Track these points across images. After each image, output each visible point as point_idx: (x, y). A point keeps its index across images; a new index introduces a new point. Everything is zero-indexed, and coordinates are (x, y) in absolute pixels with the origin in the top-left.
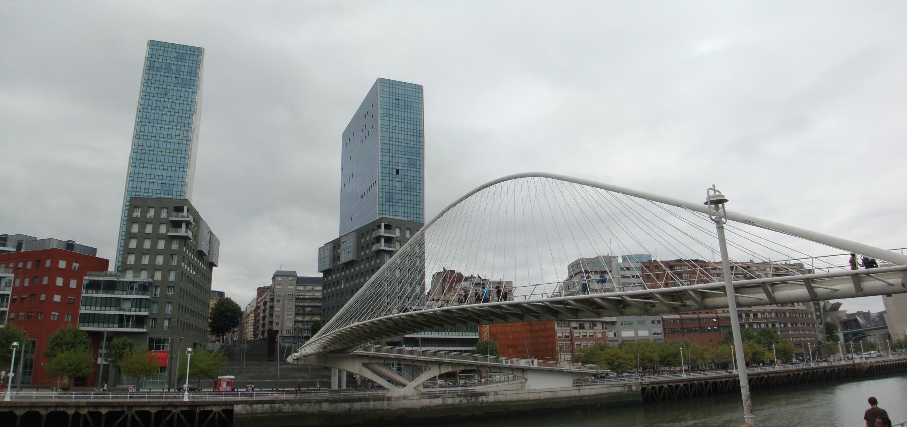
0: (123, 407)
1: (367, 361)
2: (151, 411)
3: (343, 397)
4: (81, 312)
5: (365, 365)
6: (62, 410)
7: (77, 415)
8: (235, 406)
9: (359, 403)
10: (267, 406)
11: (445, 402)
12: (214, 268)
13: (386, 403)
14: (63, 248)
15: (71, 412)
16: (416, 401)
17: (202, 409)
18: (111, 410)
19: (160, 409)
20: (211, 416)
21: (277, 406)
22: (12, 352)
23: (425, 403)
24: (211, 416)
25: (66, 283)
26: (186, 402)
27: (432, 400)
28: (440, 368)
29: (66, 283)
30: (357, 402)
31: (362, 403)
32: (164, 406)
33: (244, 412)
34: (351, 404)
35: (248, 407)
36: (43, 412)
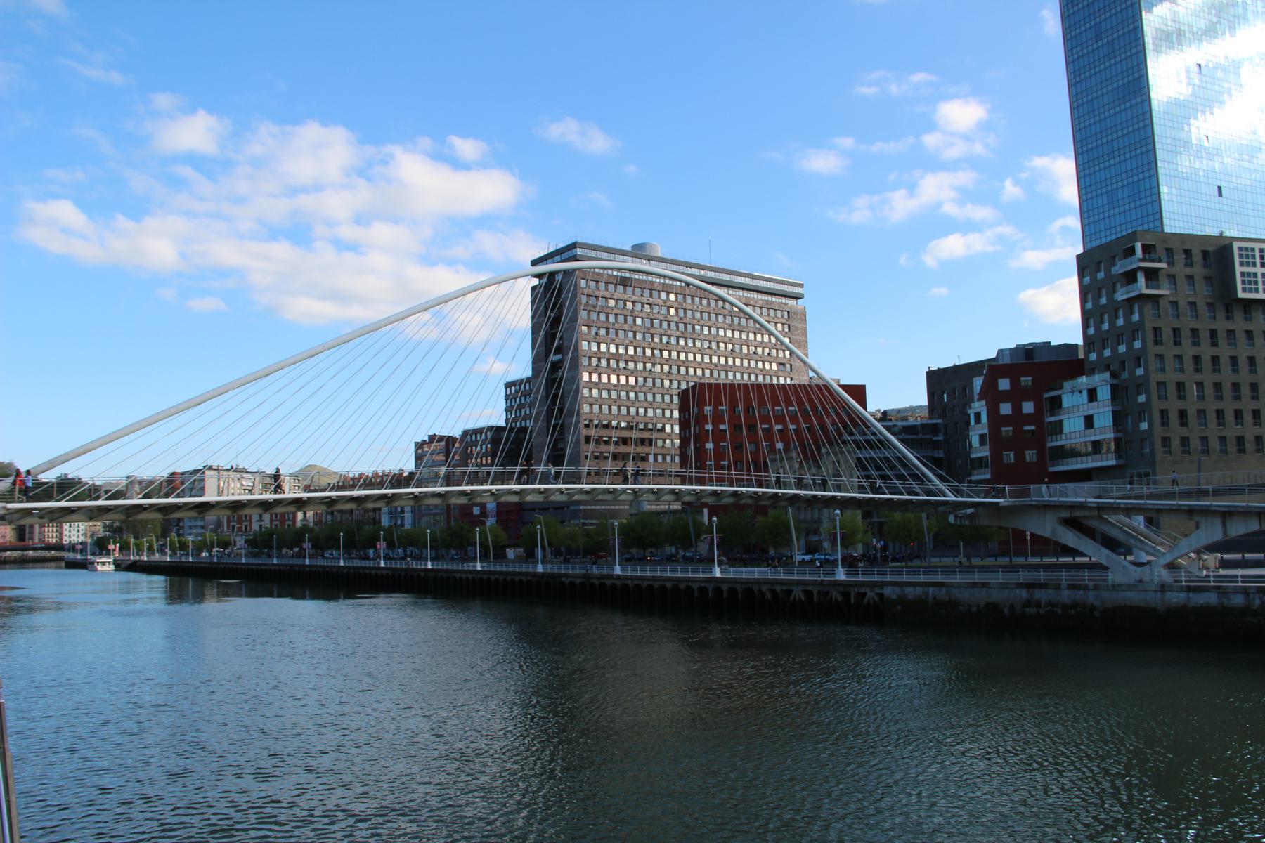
1: (1065, 514)
3: (1044, 580)
4: (1049, 445)
8: (885, 588)
9: (1043, 591)
10: (919, 590)
11: (1225, 601)
13: (1091, 594)
14: (1021, 360)
16: (1153, 593)
17: (856, 590)
18: (784, 588)
22: (836, 520)
23: (1175, 600)
25: (1017, 408)
26: (841, 581)
27: (1191, 595)
28: (1224, 525)
29: (1017, 408)
31: (1050, 591)
33: (894, 597)
35: (897, 589)
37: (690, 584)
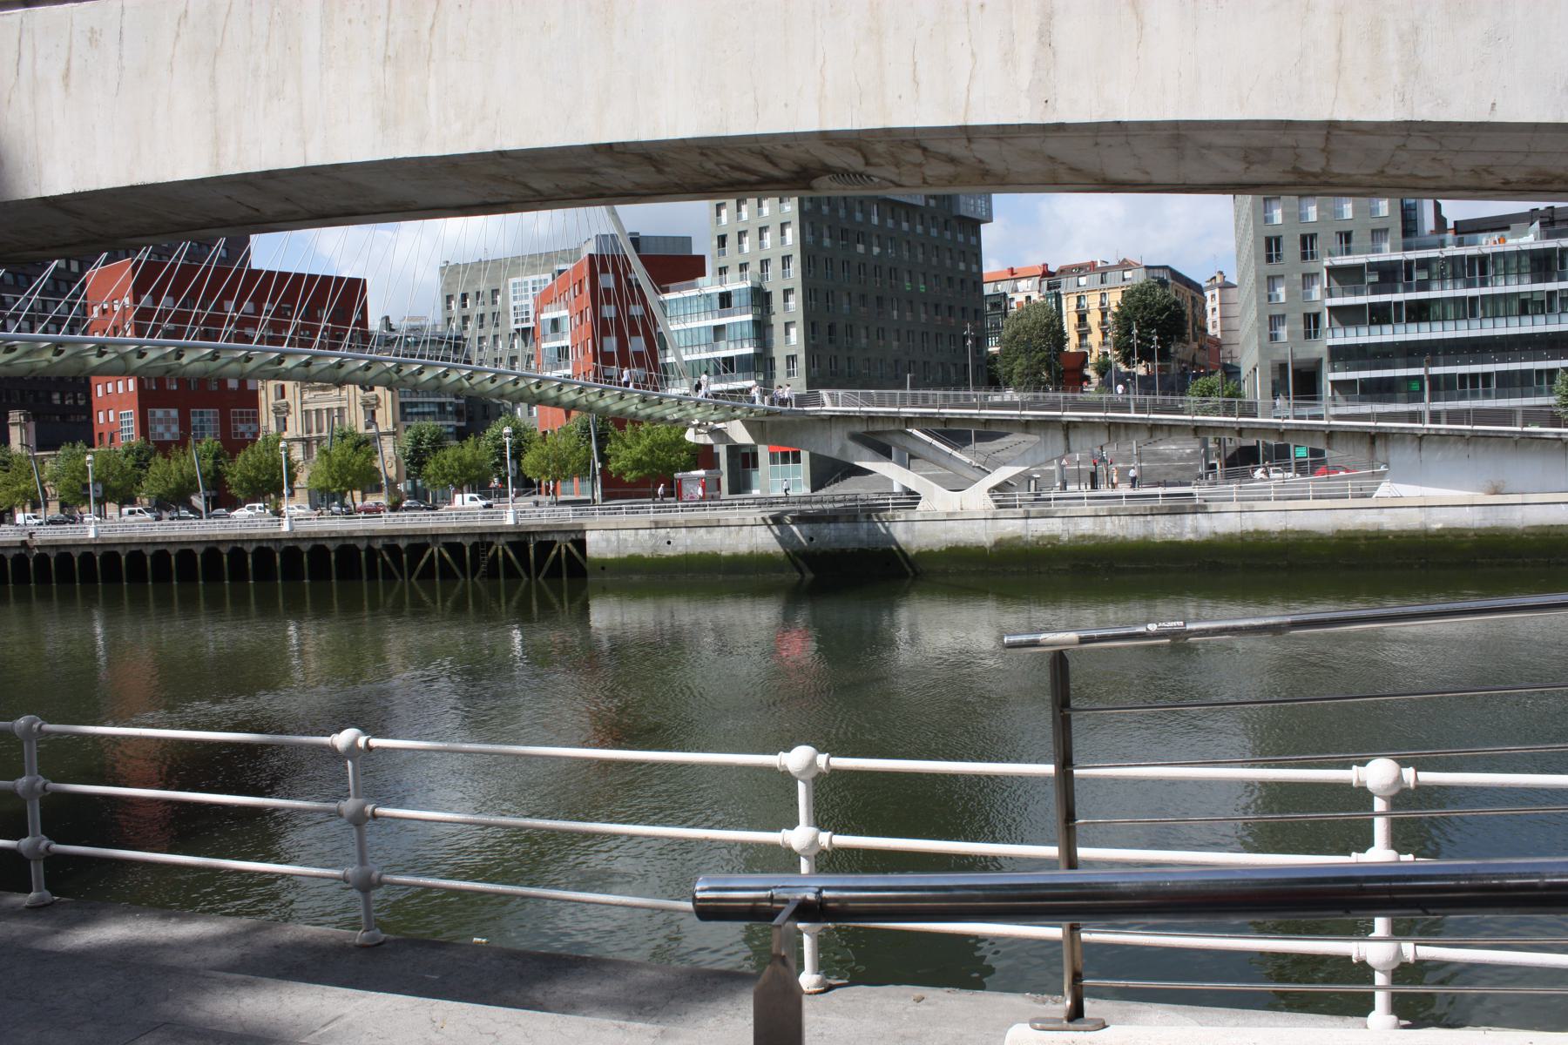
0: (426, 536)
1: (859, 428)
2: (463, 542)
5: (855, 437)
6: (352, 542)
7: (370, 550)
9: (832, 526)
12: (983, 227)
15: (362, 545)
17: (538, 539)
18: (411, 541)
19: (477, 539)
20: (554, 552)
21: (663, 532)
24: (554, 552)
28: (1067, 438)
30: (829, 522)
31: (841, 526)
32: (481, 535)
34: (816, 527)
36: (331, 545)
37: (239, 545)
